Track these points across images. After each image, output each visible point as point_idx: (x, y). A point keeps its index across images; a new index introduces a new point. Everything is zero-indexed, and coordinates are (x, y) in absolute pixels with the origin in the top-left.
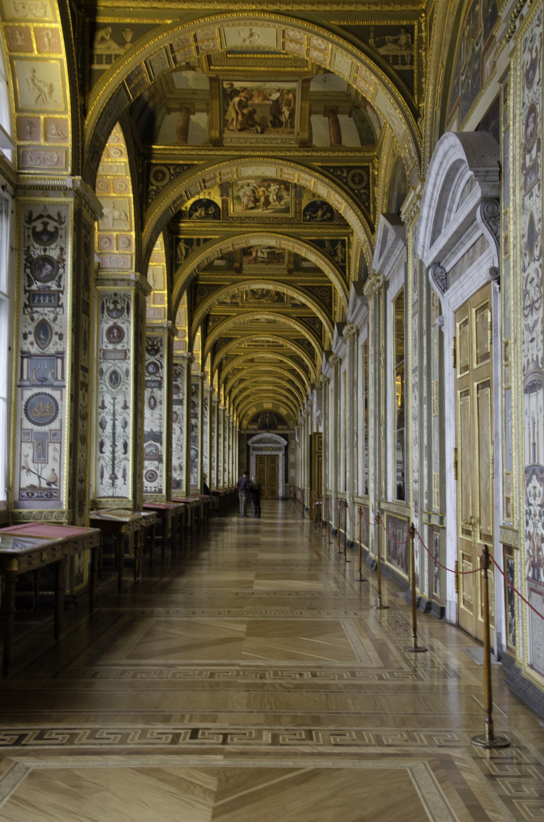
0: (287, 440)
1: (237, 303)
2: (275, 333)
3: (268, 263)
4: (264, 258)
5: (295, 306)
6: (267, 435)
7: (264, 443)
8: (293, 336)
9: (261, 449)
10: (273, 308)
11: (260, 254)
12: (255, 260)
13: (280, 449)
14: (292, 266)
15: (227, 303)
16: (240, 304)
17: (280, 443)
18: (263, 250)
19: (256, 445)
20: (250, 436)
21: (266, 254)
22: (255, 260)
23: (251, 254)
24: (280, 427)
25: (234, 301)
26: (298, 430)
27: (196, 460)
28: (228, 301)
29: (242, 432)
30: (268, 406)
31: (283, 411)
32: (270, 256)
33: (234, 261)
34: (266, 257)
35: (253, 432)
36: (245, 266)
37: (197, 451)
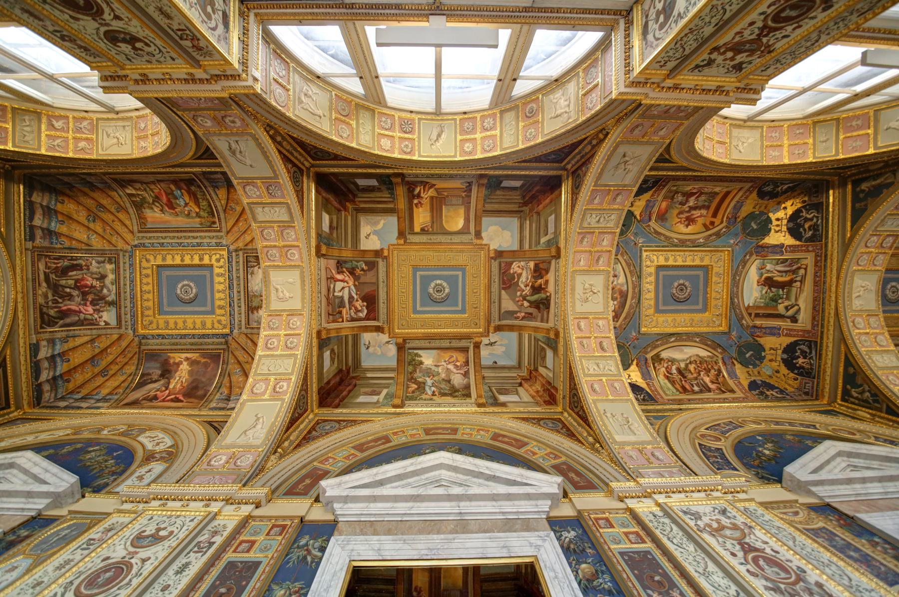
1: (32, 238)
3: (328, 299)
4: (334, 291)
5: (35, 349)
10: (26, 309)
11: (339, 285)
12: (331, 279)
14: (324, 336)
15: (31, 218)
16: (29, 245)
18: (346, 291)
21: (340, 294)
22: (331, 279)
23: (338, 273)
25: (38, 233)
28: (38, 221)
32: (337, 301)
33: (328, 245)
34: (336, 294)
36: (323, 261)
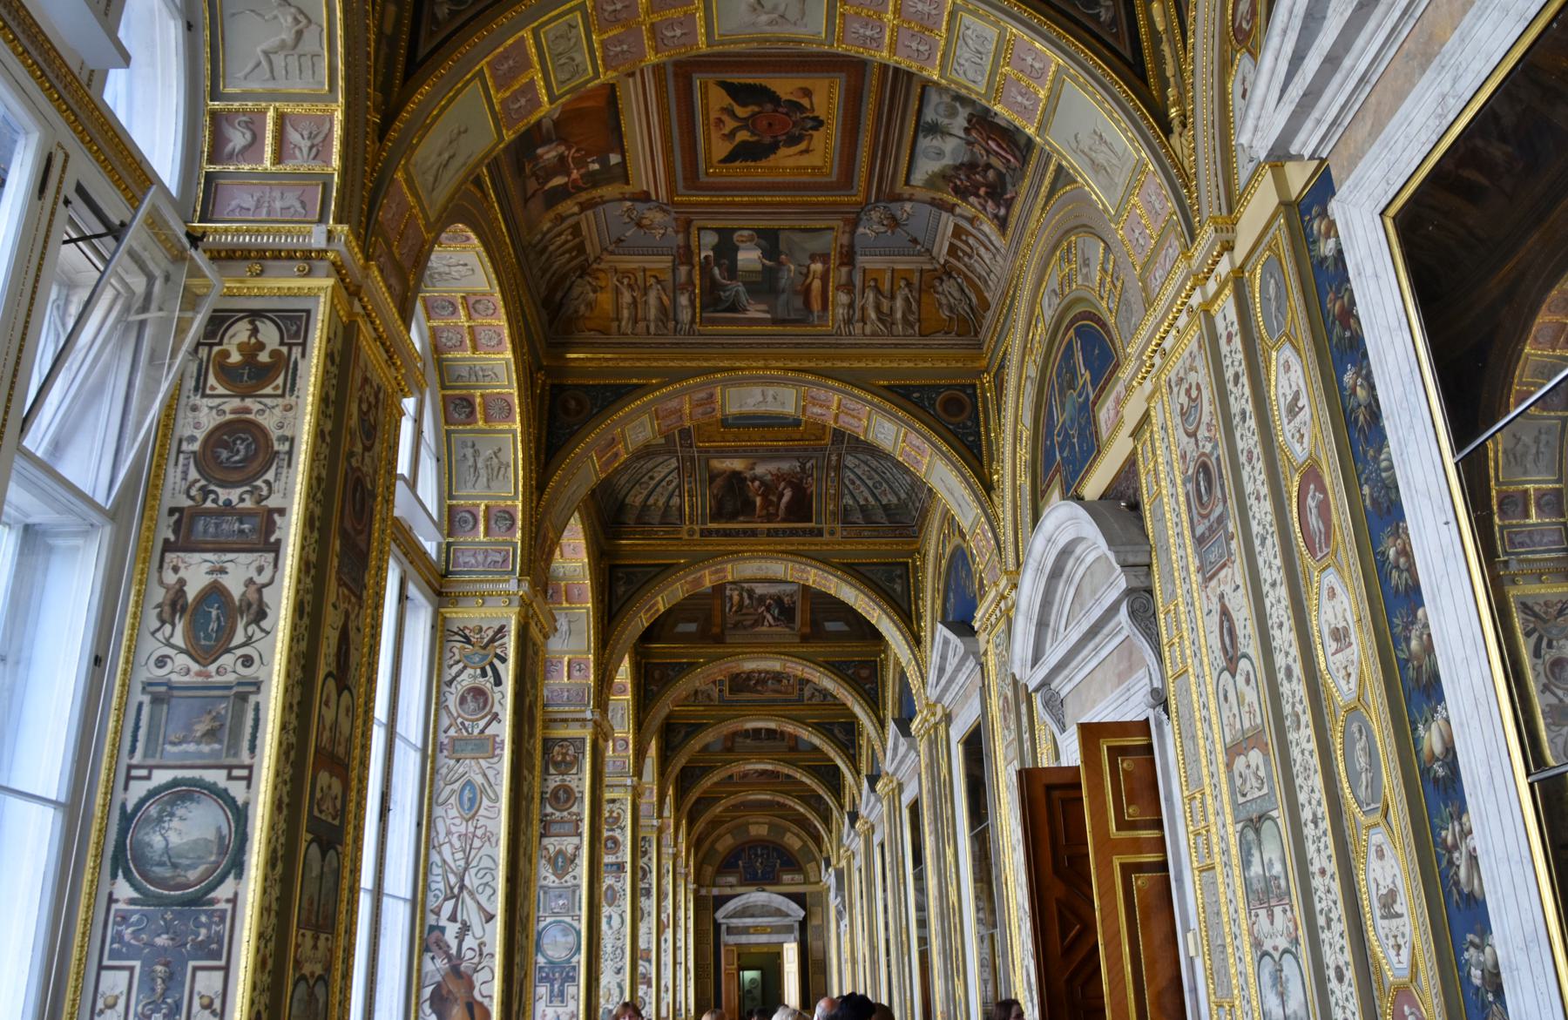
0: (803, 906)
2: (806, 364)
6: (757, 897)
7: (752, 916)
8: (881, 373)
9: (745, 930)
13: (788, 929)
17: (788, 915)
19: (735, 922)
20: (721, 901)
24: (786, 878)
26: (839, 875)
27: (224, 891)
29: (703, 892)
30: (759, 830)
31: (793, 841)
35: (728, 891)
37: (240, 815)
